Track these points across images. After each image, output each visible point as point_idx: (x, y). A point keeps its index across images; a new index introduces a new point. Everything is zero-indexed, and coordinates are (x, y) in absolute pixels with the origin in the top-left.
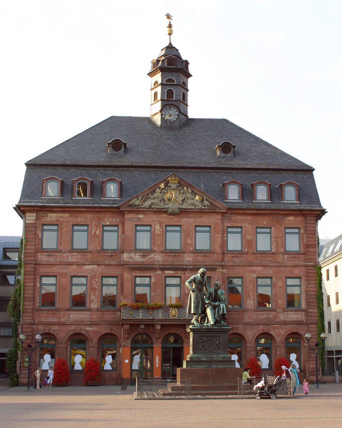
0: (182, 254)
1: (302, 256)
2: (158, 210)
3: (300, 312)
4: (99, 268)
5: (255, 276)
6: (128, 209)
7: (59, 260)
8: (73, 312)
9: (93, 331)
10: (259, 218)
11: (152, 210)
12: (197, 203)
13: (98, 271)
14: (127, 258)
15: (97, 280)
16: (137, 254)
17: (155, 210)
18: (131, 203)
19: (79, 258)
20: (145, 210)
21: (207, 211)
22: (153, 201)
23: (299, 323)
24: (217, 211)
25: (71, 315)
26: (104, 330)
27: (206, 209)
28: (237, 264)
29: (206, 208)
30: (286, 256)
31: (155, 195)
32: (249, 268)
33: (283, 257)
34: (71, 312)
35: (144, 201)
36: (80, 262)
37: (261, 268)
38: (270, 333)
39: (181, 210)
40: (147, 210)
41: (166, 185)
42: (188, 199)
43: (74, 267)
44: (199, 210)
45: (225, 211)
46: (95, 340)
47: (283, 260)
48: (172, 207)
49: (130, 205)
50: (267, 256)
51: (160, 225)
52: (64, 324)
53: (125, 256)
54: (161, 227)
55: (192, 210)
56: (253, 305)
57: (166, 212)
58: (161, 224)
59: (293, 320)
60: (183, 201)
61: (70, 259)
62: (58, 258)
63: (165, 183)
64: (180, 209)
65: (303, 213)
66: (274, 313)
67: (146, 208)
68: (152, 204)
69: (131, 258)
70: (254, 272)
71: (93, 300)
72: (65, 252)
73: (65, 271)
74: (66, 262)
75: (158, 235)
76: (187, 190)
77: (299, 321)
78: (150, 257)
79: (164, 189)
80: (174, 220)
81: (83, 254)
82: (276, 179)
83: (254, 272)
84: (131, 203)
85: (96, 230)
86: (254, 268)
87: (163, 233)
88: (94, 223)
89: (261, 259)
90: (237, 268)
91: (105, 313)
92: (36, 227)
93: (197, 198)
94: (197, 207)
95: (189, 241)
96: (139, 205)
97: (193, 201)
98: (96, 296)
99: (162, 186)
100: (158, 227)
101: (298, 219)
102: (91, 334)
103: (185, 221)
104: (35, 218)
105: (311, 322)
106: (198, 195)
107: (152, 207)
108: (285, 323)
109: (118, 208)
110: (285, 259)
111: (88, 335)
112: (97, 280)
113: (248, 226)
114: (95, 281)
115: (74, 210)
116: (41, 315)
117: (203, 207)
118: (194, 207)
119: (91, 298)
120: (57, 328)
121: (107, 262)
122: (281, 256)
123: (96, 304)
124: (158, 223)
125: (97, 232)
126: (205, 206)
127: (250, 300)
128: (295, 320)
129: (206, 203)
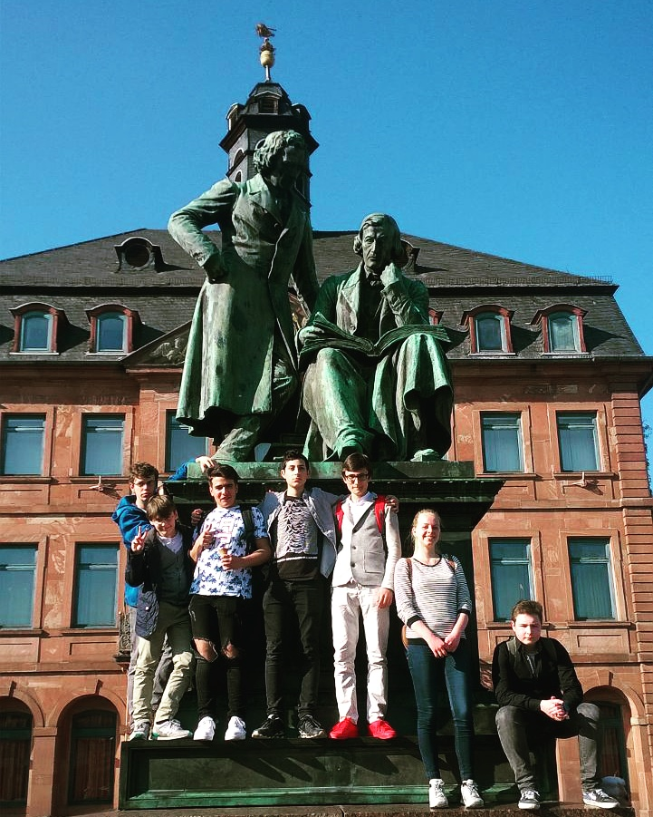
4: (70, 523)
9: (47, 691)
15: (64, 553)
18: (155, 353)
19: (18, 498)
36: (19, 508)
46: (50, 716)
49: (153, 360)
59: (595, 651)
77: (614, 655)
84: (155, 353)
85: (66, 426)
91: (82, 639)
98: (59, 593)
101: (591, 391)
102: (42, 699)
112: (64, 553)
113: (461, 410)
114: (60, 555)
123: (59, 616)
125: (69, 432)
128: (602, 651)
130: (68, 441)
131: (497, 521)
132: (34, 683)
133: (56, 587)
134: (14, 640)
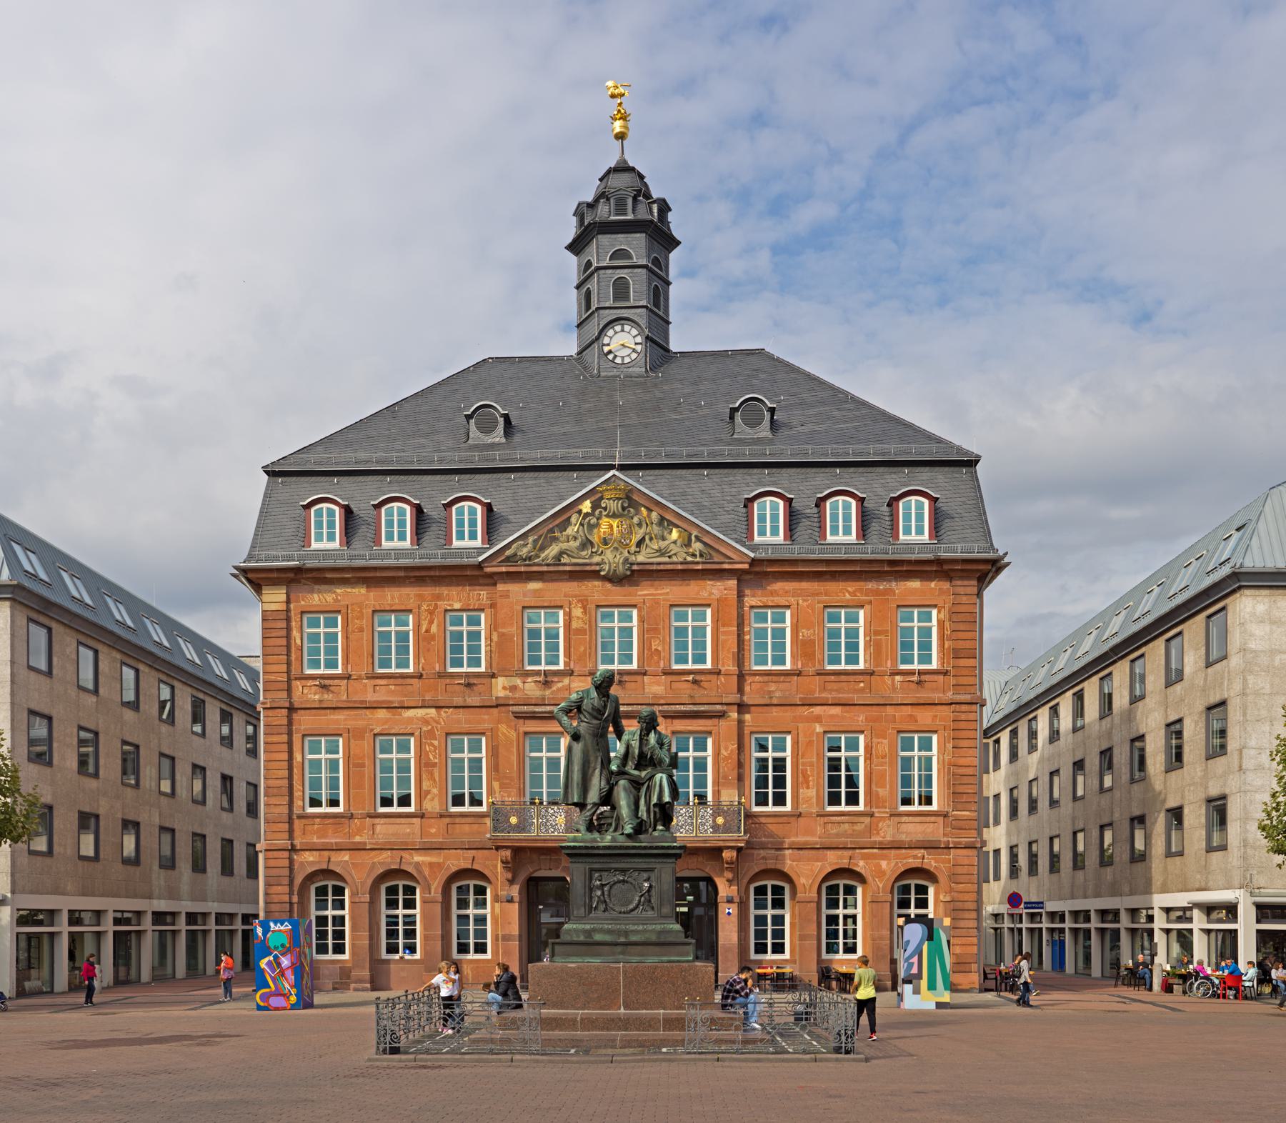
0: (638, 678)
1: (941, 677)
2: (578, 568)
3: (933, 819)
4: (439, 714)
5: (819, 729)
6: (504, 569)
7: (345, 698)
8: (383, 821)
9: (431, 865)
10: (832, 586)
11: (561, 568)
12: (674, 549)
13: (438, 723)
14: (504, 688)
15: (436, 743)
16: (530, 680)
17: (568, 568)
19: (392, 692)
20: (545, 569)
21: (700, 567)
22: (564, 546)
23: (931, 846)
24: (726, 566)
25: (378, 828)
26: (458, 861)
27: (698, 563)
28: (775, 701)
29: (698, 559)
30: (898, 678)
31: (571, 530)
32: (806, 711)
33: (893, 681)
34: (377, 820)
35: (542, 549)
37: (836, 710)
38: (858, 869)
39: (635, 567)
40: (551, 569)
41: (595, 506)
42: (651, 539)
43: (382, 714)
44: (680, 567)
45: (746, 566)
47: (894, 688)
48: (611, 560)
49: (508, 559)
50: (851, 678)
51: (584, 608)
52: (359, 848)
53: (500, 687)
54: (585, 612)
55: (662, 567)
56: (814, 800)
57: (595, 575)
58: (584, 603)
60: (639, 544)
61: (371, 697)
62: (342, 693)
63: (593, 498)
64: (632, 564)
65: (946, 567)
66: (867, 820)
67: (548, 565)
68: (561, 553)
69: (513, 688)
70: (818, 719)
71: (428, 792)
72: (359, 678)
73: (360, 723)
74: (362, 702)
75: (580, 631)
76: (649, 516)
78: (560, 685)
79: (592, 514)
80: (617, 594)
81: (400, 681)
82: (879, 486)
83: (818, 719)
85: (431, 622)
86: (817, 710)
87: (590, 626)
88: (425, 607)
89: (835, 686)
90: (774, 709)
91: (457, 820)
92: (288, 620)
93: (675, 534)
94: (674, 559)
95: (655, 645)
96: (530, 558)
97: (663, 544)
99: (586, 506)
100: (577, 612)
102: (426, 871)
103: (645, 591)
104: (284, 597)
105: (960, 843)
106: (677, 526)
107: (563, 561)
108: (897, 846)
109: (480, 566)
110: (898, 685)
111: (420, 872)
112: (436, 743)
114: (432, 745)
115: (371, 574)
116: (309, 828)
117: (689, 559)
118: (667, 559)
119: (425, 787)
120: (347, 858)
121: (458, 700)
122: (888, 679)
124: (581, 601)
126: (694, 555)
127: (808, 788)
129: (697, 546)
130: (433, 638)
131: (832, 716)
132: (418, 858)
133: (432, 774)
134: (398, 820)
